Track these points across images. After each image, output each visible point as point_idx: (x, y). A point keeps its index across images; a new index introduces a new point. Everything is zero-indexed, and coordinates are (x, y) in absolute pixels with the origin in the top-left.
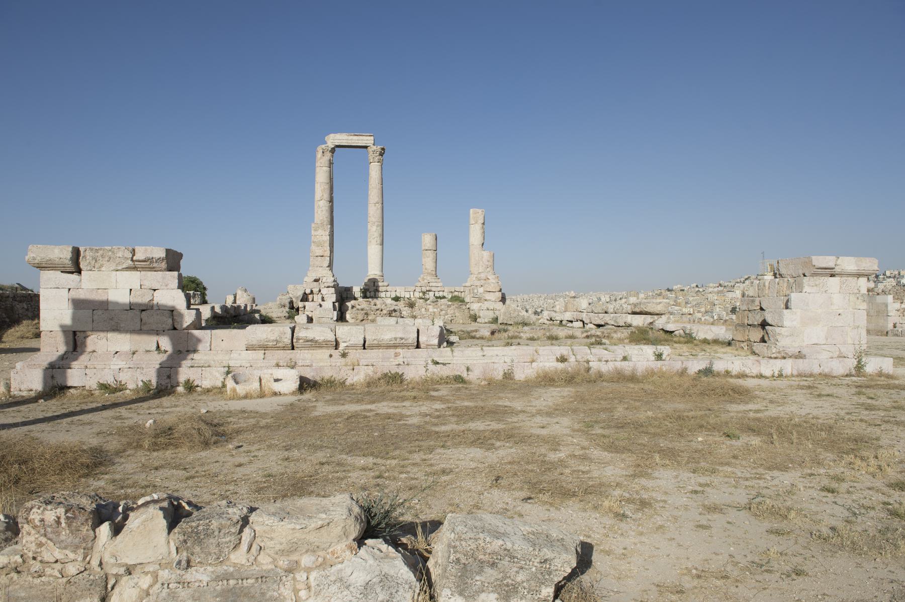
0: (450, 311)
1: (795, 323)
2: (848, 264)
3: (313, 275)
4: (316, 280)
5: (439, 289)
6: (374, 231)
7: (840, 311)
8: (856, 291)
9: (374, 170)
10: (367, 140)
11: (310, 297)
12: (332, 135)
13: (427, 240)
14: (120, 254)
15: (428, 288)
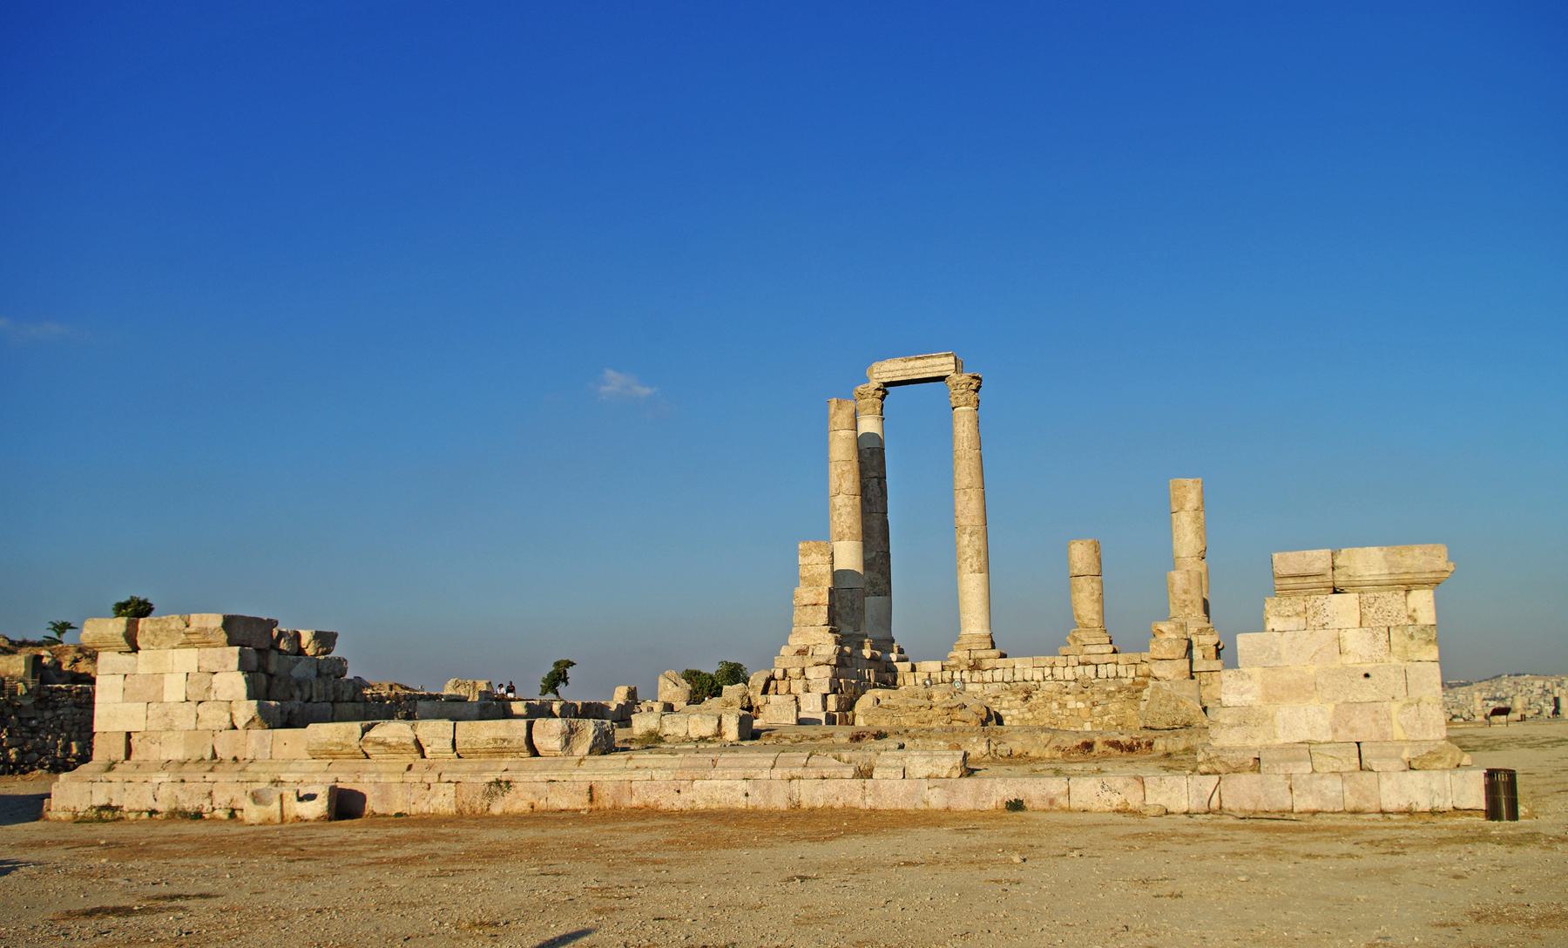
0: (1114, 707)
1: (1249, 698)
2: (1367, 562)
3: (796, 641)
4: (802, 652)
5: (1107, 658)
6: (969, 545)
7: (1367, 668)
8: (1404, 621)
9: (964, 423)
10: (941, 364)
11: (783, 687)
12: (876, 366)
13: (1080, 555)
14: (173, 627)
15: (1081, 659)
